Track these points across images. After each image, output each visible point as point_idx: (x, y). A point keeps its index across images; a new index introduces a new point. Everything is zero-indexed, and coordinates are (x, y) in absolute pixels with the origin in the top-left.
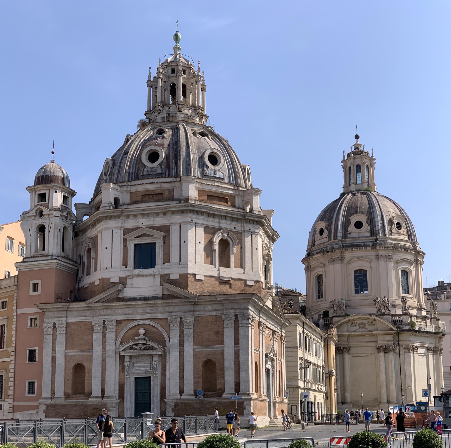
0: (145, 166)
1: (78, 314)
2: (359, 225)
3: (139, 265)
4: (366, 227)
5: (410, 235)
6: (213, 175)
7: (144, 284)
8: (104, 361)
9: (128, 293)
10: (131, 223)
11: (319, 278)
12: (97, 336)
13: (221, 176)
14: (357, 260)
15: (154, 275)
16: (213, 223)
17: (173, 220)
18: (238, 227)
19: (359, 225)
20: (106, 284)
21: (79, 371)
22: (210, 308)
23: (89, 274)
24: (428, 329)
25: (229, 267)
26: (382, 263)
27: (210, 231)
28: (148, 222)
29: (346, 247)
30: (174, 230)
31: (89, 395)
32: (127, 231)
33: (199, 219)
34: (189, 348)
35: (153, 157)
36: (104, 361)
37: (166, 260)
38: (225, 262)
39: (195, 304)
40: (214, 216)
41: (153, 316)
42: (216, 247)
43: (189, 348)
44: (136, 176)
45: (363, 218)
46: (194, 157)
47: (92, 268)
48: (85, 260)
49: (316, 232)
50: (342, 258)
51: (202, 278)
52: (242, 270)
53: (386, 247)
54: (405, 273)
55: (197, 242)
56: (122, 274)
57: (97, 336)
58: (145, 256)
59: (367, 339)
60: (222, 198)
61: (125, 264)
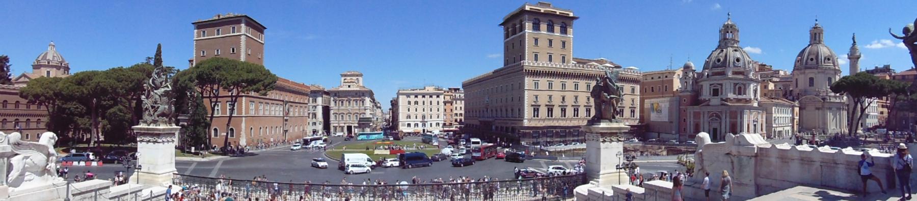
1: (697, 108)
2: (812, 59)
3: (714, 95)
4: (815, 60)
5: (834, 63)
7: (715, 101)
14: (810, 74)
17: (724, 82)
20: (705, 101)
29: (806, 68)
34: (728, 120)
35: (719, 60)
38: (740, 94)
44: (714, 67)
45: (814, 57)
46: (732, 60)
49: (797, 61)
53: (822, 68)
58: (716, 93)
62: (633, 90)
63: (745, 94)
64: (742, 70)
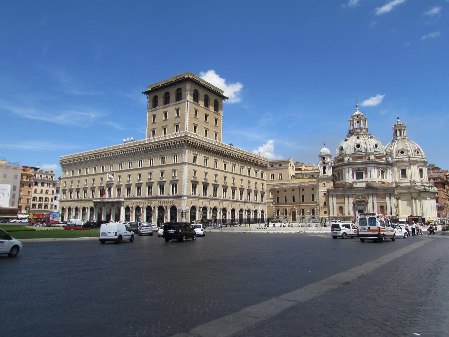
0: (355, 149)
12: (346, 199)
15: (363, 182)
16: (379, 166)
19: (402, 153)
23: (339, 180)
24: (430, 191)
26: (412, 167)
27: (378, 168)
32: (353, 169)
33: (376, 165)
34: (375, 202)
35: (358, 146)
37: (366, 177)
39: (376, 190)
43: (375, 202)
47: (340, 179)
48: (337, 176)
50: (396, 165)
54: (421, 170)
57: (346, 199)
59: (407, 194)
60: (380, 158)
61: (353, 178)
63: (386, 178)
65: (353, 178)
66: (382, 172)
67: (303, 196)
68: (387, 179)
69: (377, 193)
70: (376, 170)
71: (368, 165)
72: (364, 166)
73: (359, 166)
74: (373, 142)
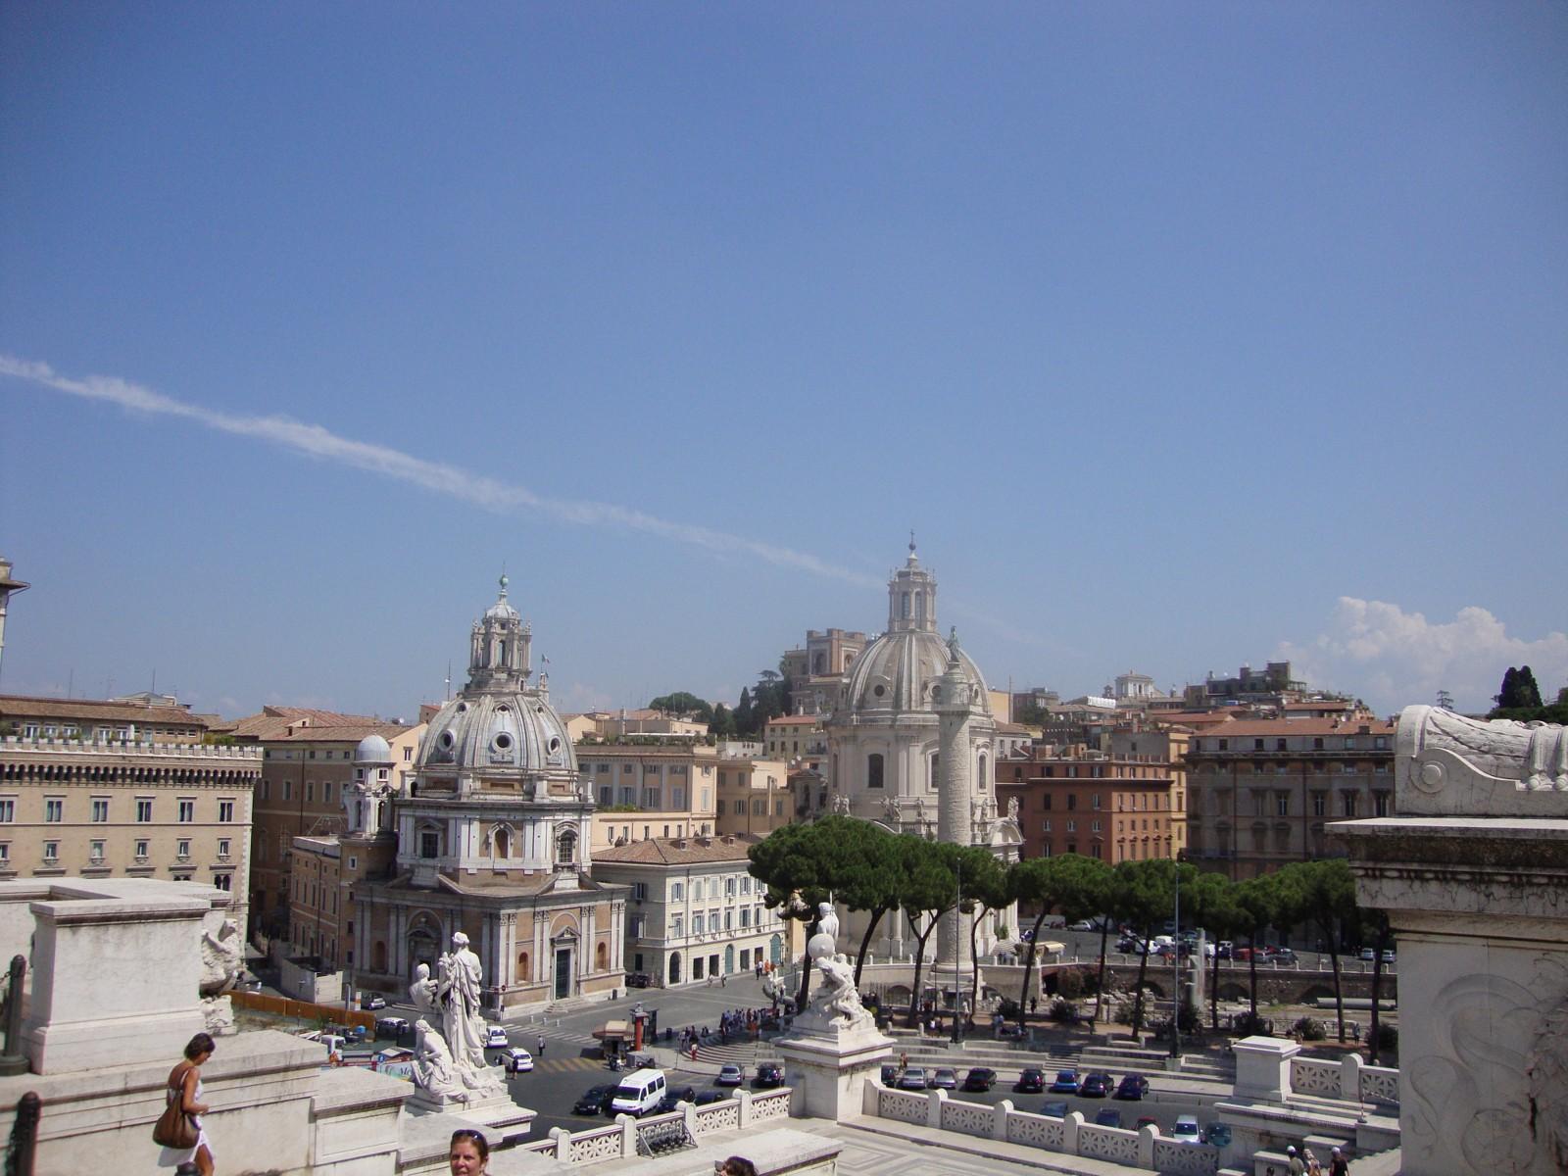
6: (500, 759)
8: (397, 942)
9: (418, 880)
10: (420, 813)
11: (836, 756)
12: (393, 918)
13: (510, 759)
18: (519, 817)
21: (381, 948)
22: (474, 904)
25: (506, 857)
28: (432, 813)
30: (452, 823)
31: (386, 972)
32: (418, 820)
36: (397, 942)
37: (445, 853)
40: (491, 809)
41: (432, 906)
42: (492, 840)
50: (855, 738)
51: (475, 872)
52: (521, 860)
55: (471, 837)
56: (413, 862)
57: (393, 918)
60: (506, 784)
61: (415, 851)
62: (226, 810)
63: (520, 853)
64: (512, 772)
65: (415, 851)
66: (502, 838)
67: (324, 890)
68: (518, 860)
69: (464, 908)
70: (476, 825)
71: (452, 814)
72: (442, 814)
73: (432, 813)
74: (506, 724)
